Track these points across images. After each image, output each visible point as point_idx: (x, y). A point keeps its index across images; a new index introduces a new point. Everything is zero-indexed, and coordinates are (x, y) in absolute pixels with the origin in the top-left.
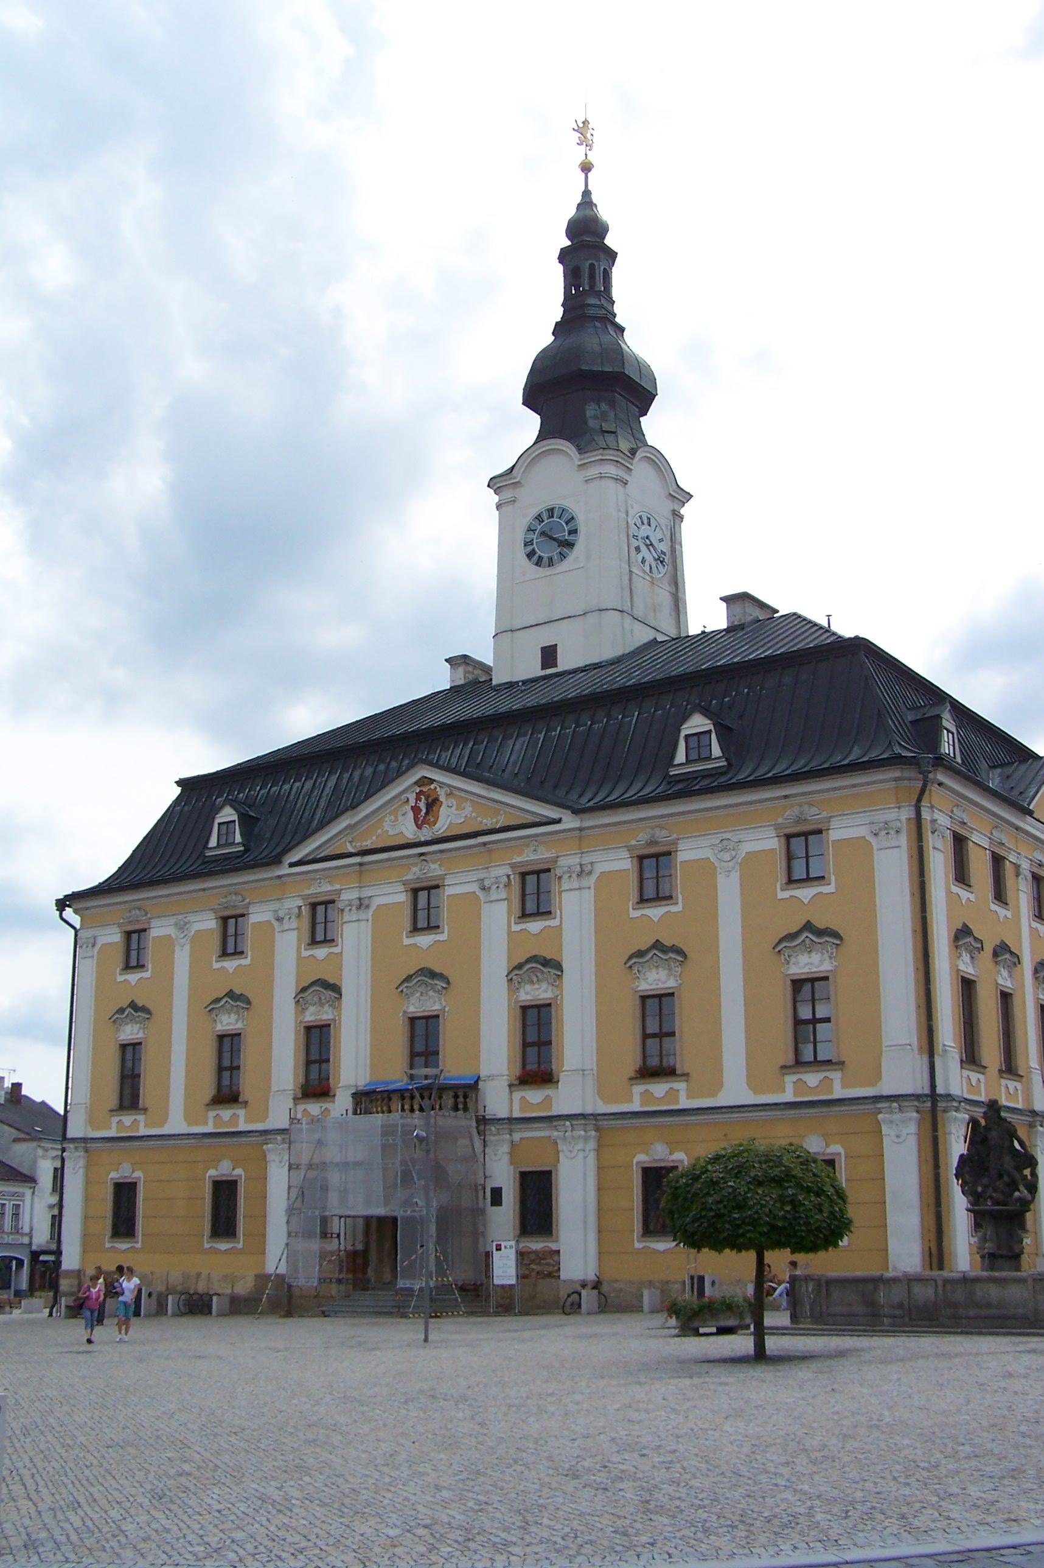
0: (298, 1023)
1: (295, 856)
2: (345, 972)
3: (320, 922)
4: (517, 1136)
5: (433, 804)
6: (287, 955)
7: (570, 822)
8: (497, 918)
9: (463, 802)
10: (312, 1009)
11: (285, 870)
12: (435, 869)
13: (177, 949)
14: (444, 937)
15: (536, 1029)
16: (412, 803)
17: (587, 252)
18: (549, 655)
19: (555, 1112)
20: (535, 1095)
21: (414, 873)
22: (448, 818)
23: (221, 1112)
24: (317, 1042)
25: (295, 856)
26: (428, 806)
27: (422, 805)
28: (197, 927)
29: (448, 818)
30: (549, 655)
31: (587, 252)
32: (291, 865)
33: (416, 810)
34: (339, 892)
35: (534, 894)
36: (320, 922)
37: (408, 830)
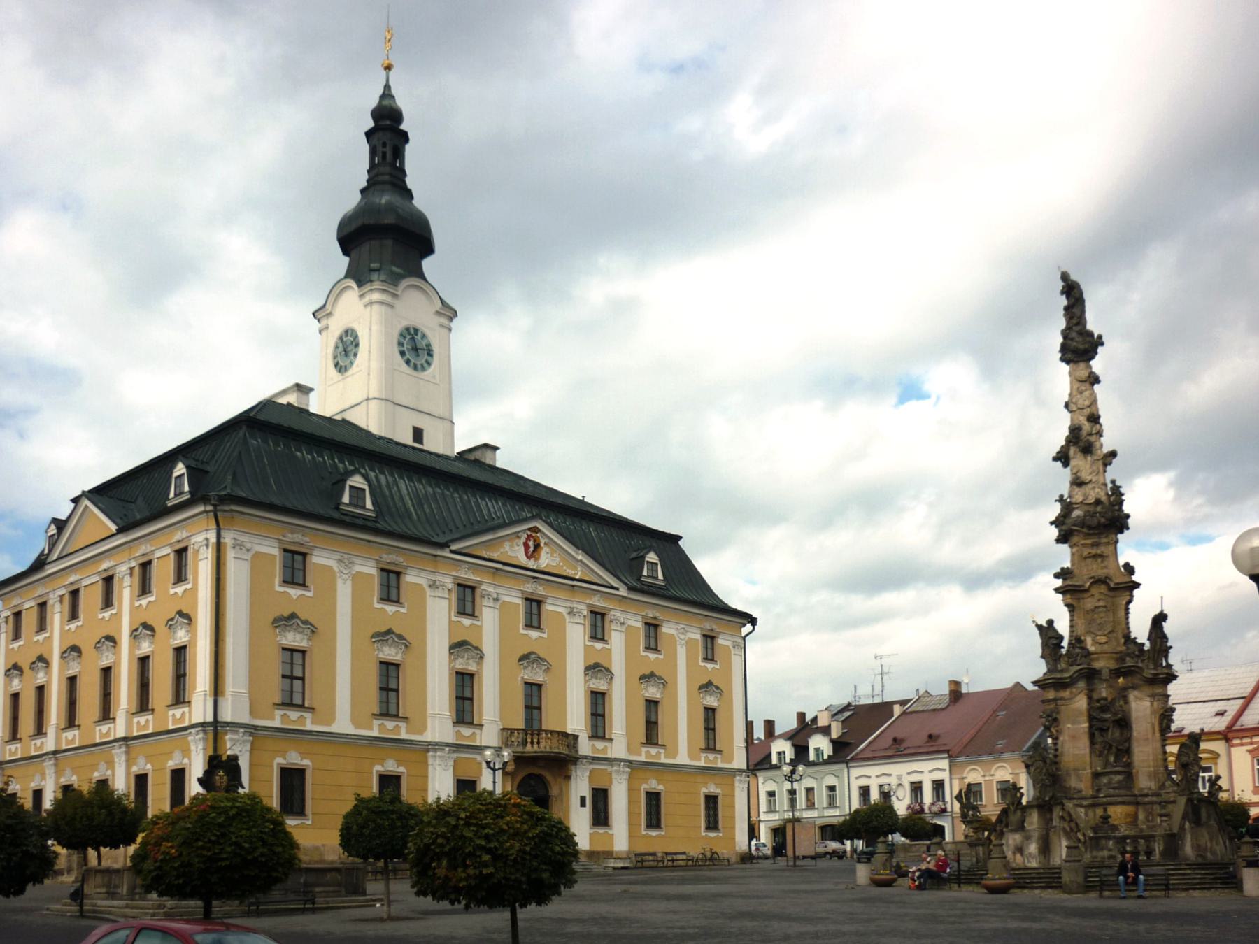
0: (451, 669)
1: (454, 547)
2: (484, 638)
4: (592, 767)
5: (537, 546)
6: (438, 618)
7: (623, 592)
8: (576, 635)
9: (556, 554)
10: (460, 660)
11: (446, 553)
12: (540, 590)
13: (339, 583)
14: (545, 636)
16: (523, 540)
17: (387, 132)
18: (418, 434)
19: (609, 756)
20: (600, 745)
21: (529, 587)
22: (546, 560)
23: (288, 713)
24: (464, 685)
25: (454, 547)
27: (531, 543)
28: (358, 568)
29: (546, 560)
30: (418, 434)
31: (387, 132)
32: (452, 552)
33: (526, 546)
34: (481, 583)
35: (598, 624)
37: (522, 559)
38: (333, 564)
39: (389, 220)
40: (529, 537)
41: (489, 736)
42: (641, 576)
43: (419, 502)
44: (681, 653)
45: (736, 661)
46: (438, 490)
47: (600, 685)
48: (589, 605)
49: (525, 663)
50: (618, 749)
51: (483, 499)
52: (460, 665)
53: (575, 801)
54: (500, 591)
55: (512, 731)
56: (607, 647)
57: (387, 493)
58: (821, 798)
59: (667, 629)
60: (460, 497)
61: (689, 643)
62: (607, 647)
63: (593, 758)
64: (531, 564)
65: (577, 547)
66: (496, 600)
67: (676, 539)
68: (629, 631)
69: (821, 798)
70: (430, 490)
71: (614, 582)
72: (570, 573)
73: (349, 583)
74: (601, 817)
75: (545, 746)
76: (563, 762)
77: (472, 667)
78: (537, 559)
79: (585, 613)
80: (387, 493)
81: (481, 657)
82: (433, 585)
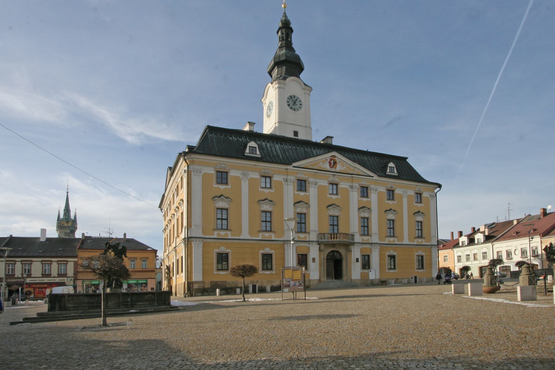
0: (295, 212)
3: (302, 185)
5: (335, 163)
6: (290, 192)
7: (376, 177)
12: (336, 180)
13: (243, 182)
14: (339, 197)
15: (365, 224)
21: (331, 179)
26: (333, 163)
27: (332, 162)
29: (339, 168)
33: (330, 163)
35: (365, 191)
36: (302, 185)
37: (327, 167)
38: (240, 175)
39: (283, 58)
40: (331, 160)
41: (313, 237)
42: (386, 172)
43: (284, 151)
44: (405, 201)
45: (432, 202)
46: (294, 147)
47: (366, 215)
48: (359, 184)
49: (330, 208)
50: (375, 239)
51: (314, 149)
52: (299, 210)
53: (353, 260)
54: (317, 180)
55: (324, 234)
56: (369, 200)
57: (270, 149)
58: (480, 256)
59: (398, 191)
60: (304, 149)
61: (409, 197)
62: (369, 200)
63: (362, 243)
64: (333, 170)
65: (354, 162)
66: (316, 184)
67: (405, 159)
68: (380, 193)
69: (480, 256)
70: (290, 147)
71: (371, 174)
72: (351, 172)
73: (247, 182)
74: (366, 265)
75: (340, 239)
76: (348, 246)
77: (304, 211)
78: (335, 168)
79: (358, 187)
80: (270, 149)
81: (309, 207)
82: (286, 180)
